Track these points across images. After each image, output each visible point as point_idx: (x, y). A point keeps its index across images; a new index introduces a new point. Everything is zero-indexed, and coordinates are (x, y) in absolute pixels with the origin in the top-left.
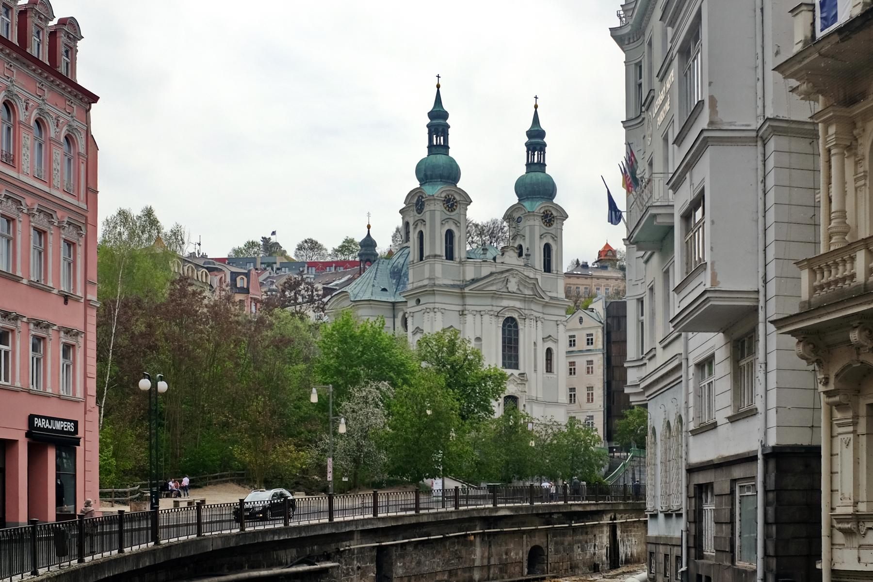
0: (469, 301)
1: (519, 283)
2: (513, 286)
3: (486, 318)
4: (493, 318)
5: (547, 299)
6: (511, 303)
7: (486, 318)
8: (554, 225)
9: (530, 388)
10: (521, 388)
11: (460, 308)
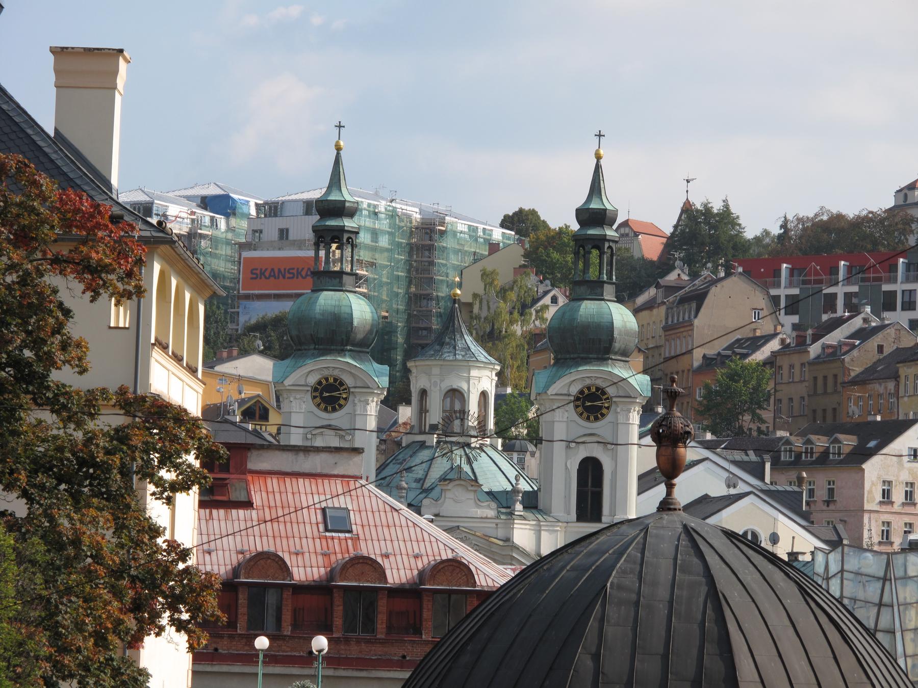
8: (609, 418)
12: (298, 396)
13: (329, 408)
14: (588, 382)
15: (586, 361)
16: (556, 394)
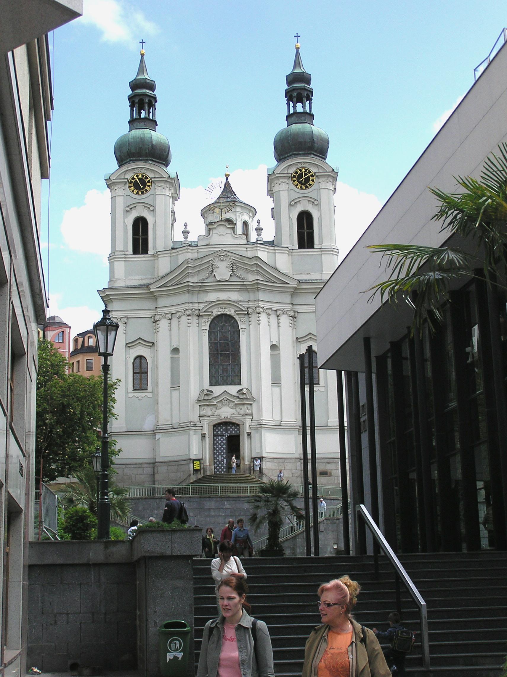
0: (162, 302)
1: (233, 267)
2: (223, 272)
3: (184, 319)
4: (195, 320)
5: (294, 284)
6: (223, 296)
7: (184, 319)
8: (315, 186)
9: (260, 410)
10: (244, 410)
11: (152, 313)
12: (119, 186)
13: (140, 192)
14: (300, 166)
15: (298, 155)
16: (280, 173)
